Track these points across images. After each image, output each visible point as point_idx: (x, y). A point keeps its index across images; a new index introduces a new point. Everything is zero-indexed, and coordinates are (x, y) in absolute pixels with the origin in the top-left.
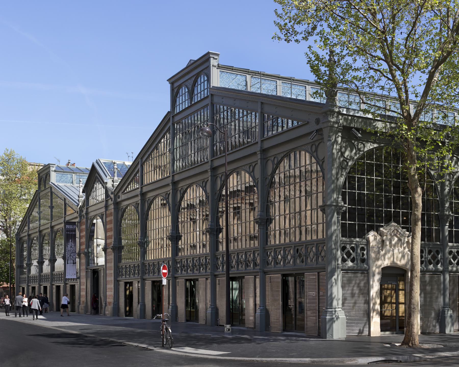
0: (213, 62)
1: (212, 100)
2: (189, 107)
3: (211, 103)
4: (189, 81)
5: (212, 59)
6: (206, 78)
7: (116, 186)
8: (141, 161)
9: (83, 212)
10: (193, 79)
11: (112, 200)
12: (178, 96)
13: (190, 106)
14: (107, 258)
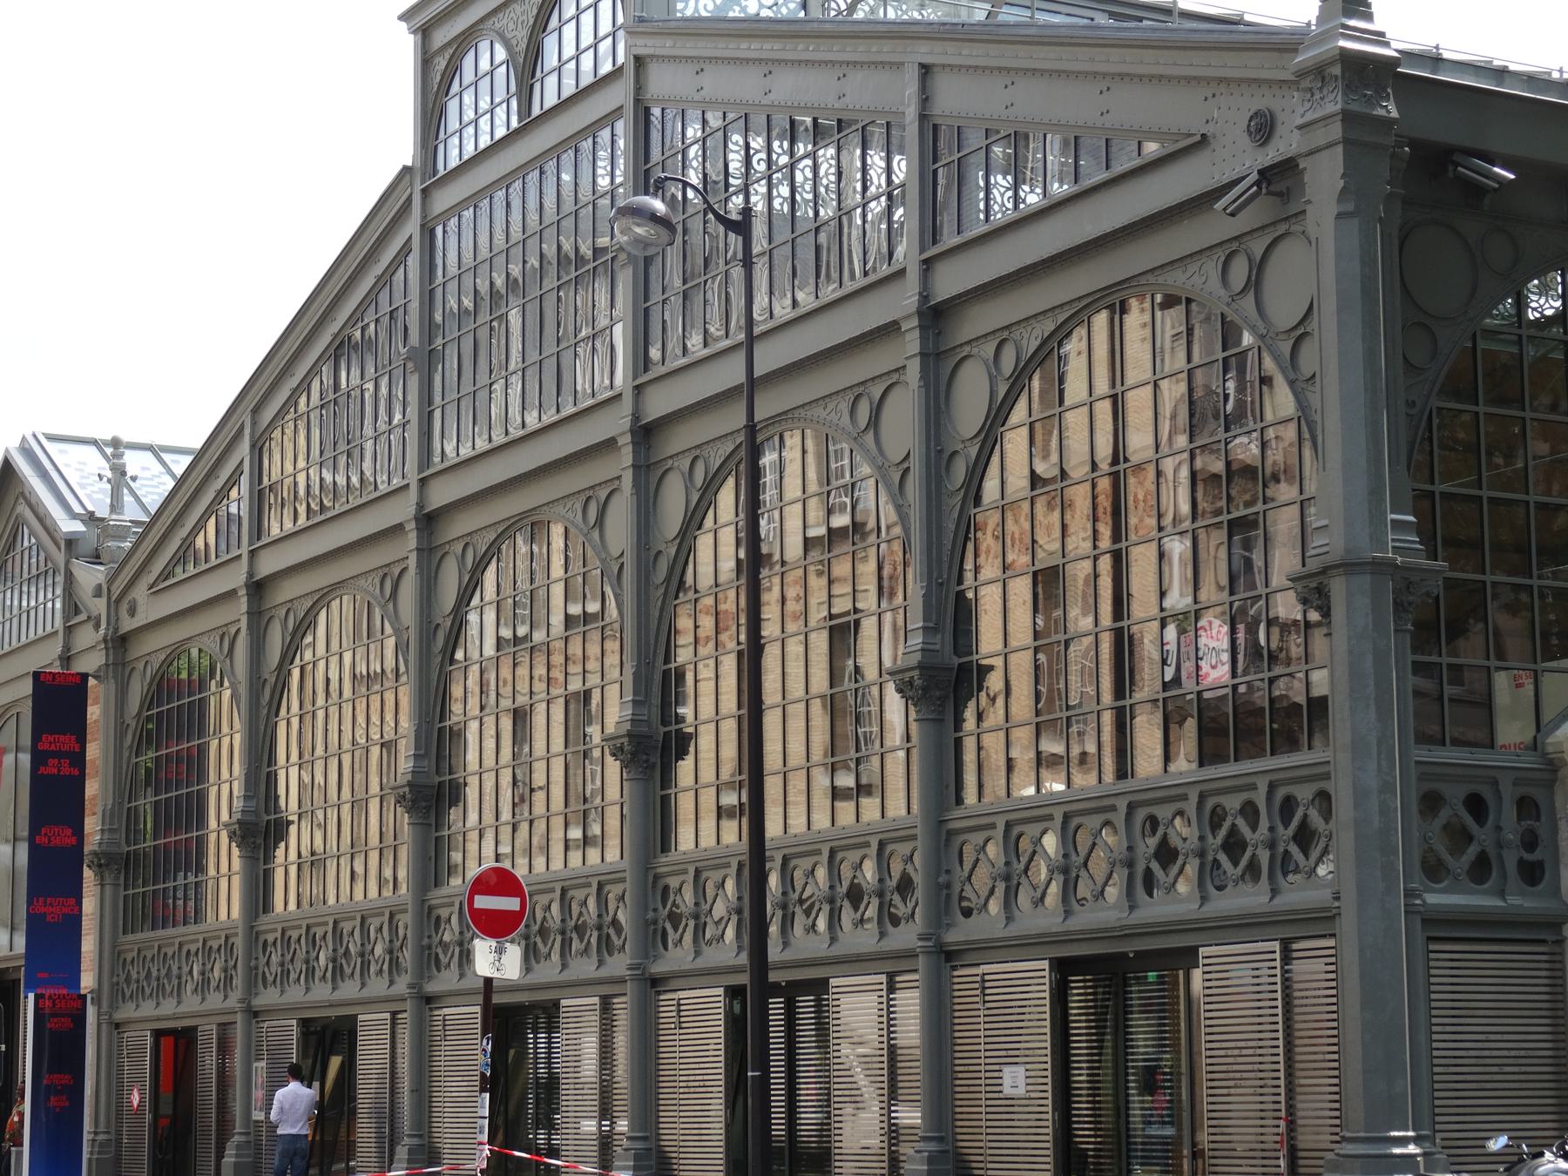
1: (639, 87)
2: (512, 137)
3: (637, 101)
8: (254, 423)
11: (97, 626)
12: (455, 88)
13: (517, 132)
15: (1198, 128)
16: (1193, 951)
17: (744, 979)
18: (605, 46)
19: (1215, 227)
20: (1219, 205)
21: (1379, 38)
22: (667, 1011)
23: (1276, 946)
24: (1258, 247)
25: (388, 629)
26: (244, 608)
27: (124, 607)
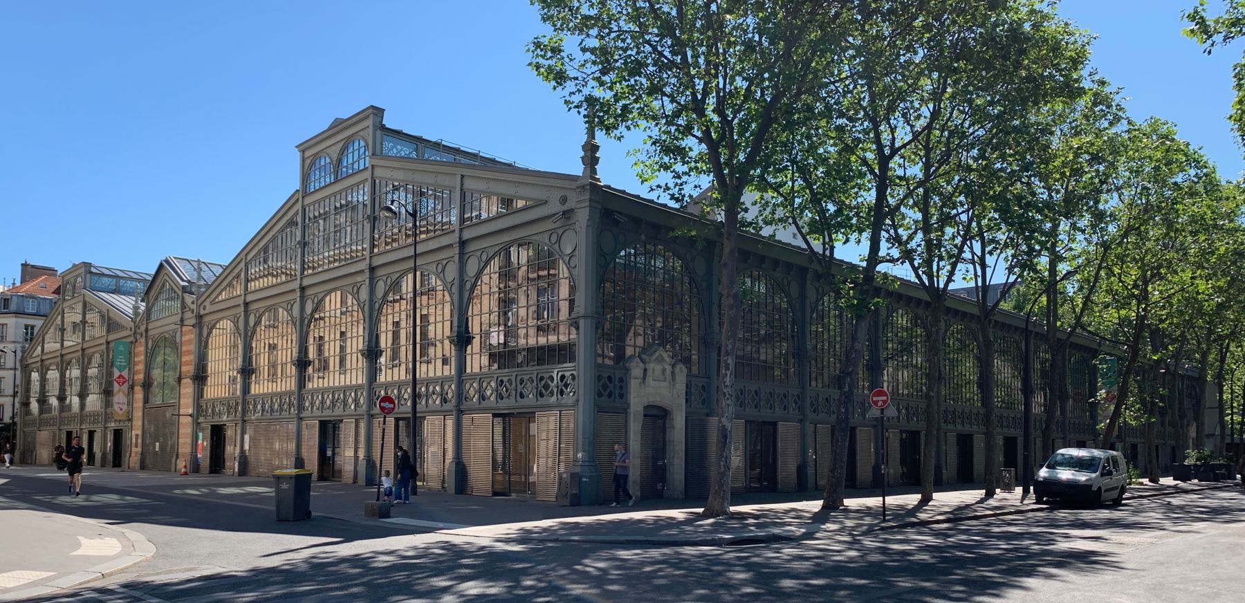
1: (373, 174)
2: (331, 184)
3: (372, 178)
4: (334, 148)
6: (362, 143)
8: (246, 259)
10: (341, 145)
11: (193, 312)
15: (544, 198)
19: (549, 225)
21: (598, 180)
24: (560, 232)
27: (202, 306)
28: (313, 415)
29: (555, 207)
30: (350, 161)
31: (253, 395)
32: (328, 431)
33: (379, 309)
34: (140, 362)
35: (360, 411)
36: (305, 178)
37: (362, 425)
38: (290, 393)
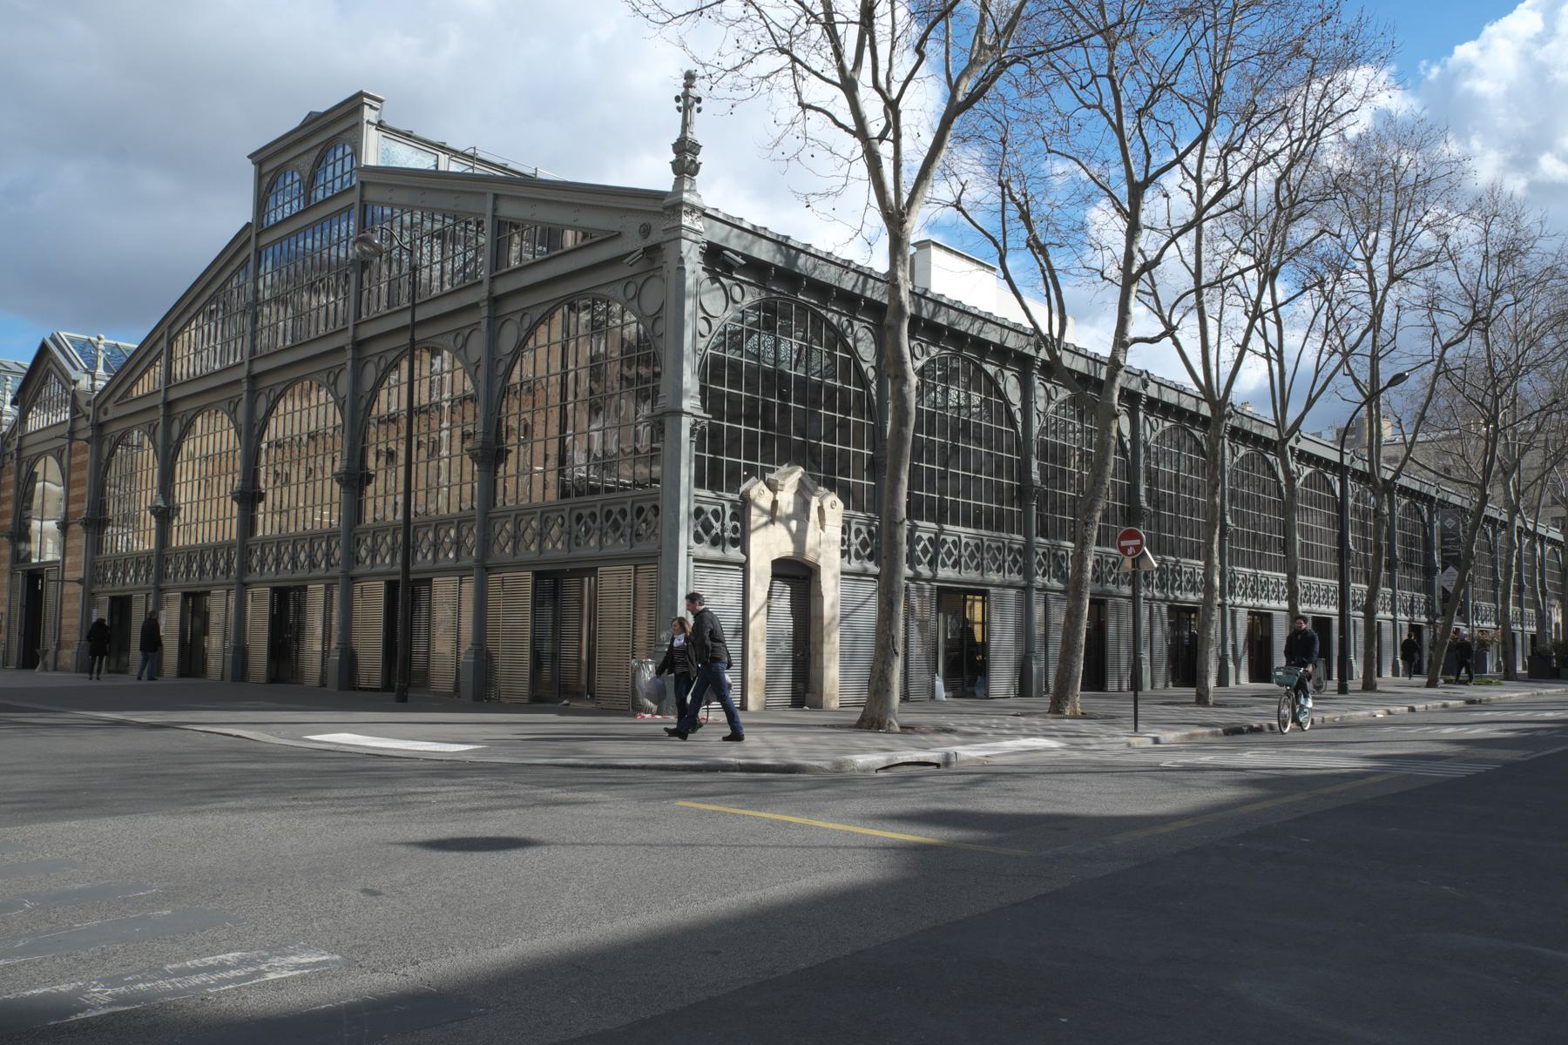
0: (369, 115)
1: (362, 196)
3: (361, 201)
4: (305, 157)
5: (366, 107)
6: (348, 149)
7: (100, 388)
8: (169, 333)
9: (9, 446)
10: (316, 152)
11: (88, 419)
12: (274, 190)
13: (303, 211)
14: (68, 546)
16: (596, 569)
17: (399, 577)
18: (346, 177)
20: (625, 261)
22: (357, 591)
23: (632, 567)
25: (231, 425)
26: (161, 413)
27: (102, 410)
28: (264, 578)
29: (633, 243)
30: (330, 177)
31: (175, 549)
32: (287, 604)
33: (367, 405)
34: (8, 498)
35: (335, 571)
36: (262, 203)
37: (337, 594)
38: (229, 546)
